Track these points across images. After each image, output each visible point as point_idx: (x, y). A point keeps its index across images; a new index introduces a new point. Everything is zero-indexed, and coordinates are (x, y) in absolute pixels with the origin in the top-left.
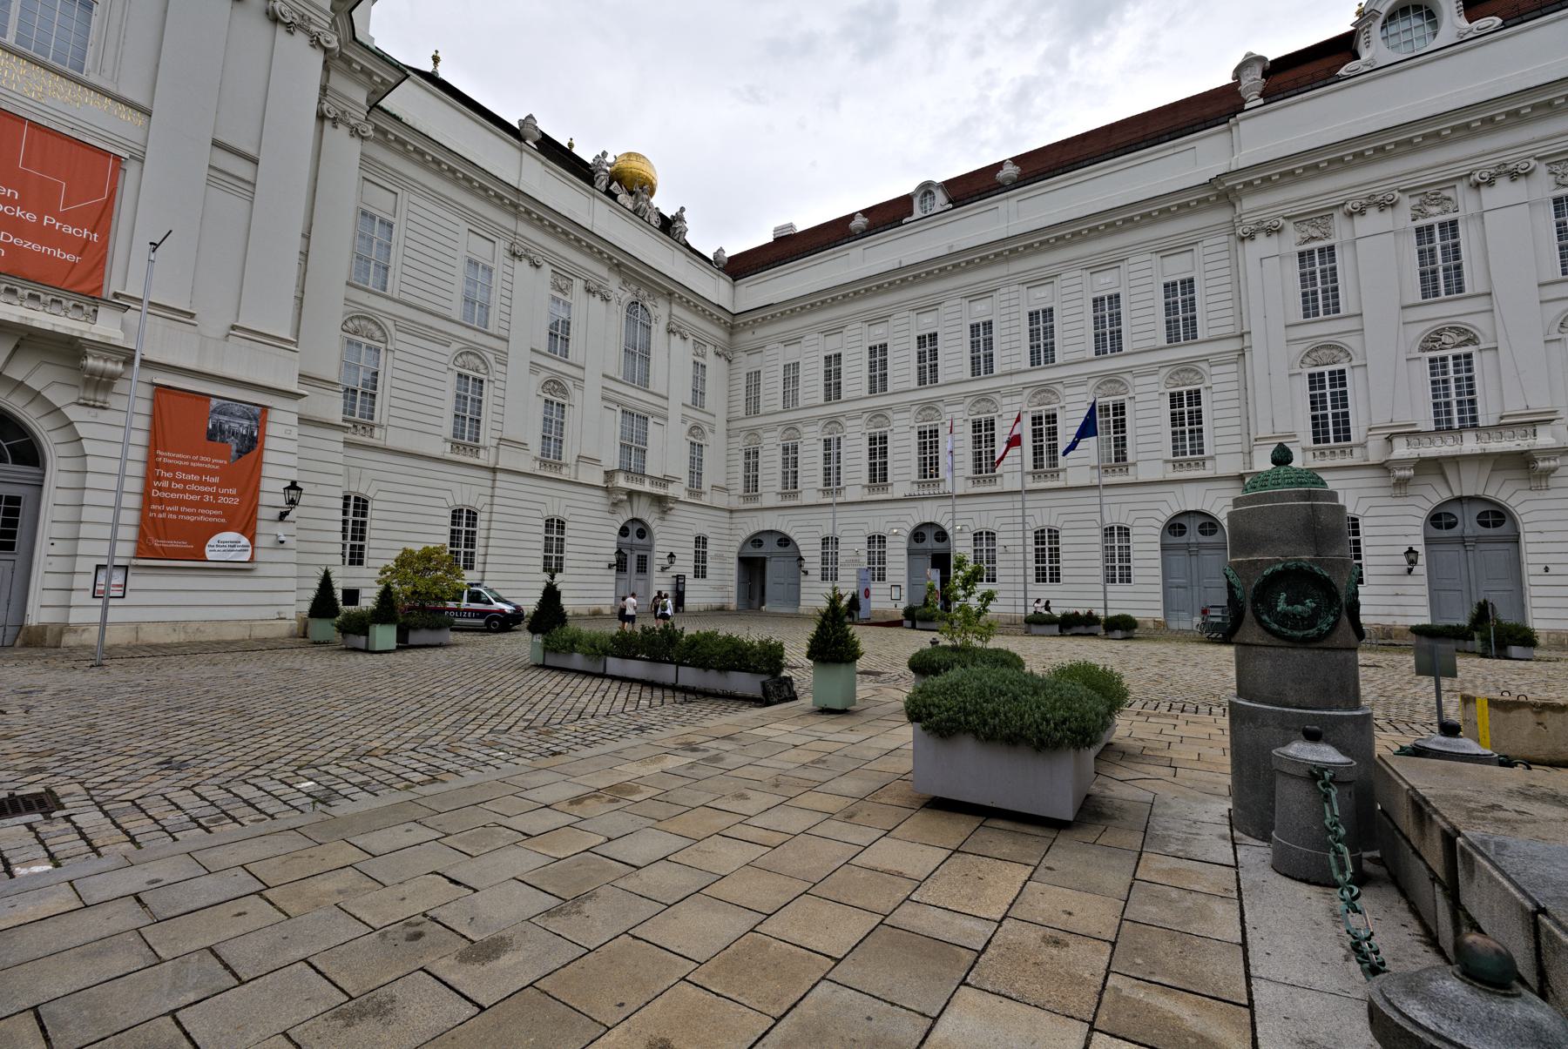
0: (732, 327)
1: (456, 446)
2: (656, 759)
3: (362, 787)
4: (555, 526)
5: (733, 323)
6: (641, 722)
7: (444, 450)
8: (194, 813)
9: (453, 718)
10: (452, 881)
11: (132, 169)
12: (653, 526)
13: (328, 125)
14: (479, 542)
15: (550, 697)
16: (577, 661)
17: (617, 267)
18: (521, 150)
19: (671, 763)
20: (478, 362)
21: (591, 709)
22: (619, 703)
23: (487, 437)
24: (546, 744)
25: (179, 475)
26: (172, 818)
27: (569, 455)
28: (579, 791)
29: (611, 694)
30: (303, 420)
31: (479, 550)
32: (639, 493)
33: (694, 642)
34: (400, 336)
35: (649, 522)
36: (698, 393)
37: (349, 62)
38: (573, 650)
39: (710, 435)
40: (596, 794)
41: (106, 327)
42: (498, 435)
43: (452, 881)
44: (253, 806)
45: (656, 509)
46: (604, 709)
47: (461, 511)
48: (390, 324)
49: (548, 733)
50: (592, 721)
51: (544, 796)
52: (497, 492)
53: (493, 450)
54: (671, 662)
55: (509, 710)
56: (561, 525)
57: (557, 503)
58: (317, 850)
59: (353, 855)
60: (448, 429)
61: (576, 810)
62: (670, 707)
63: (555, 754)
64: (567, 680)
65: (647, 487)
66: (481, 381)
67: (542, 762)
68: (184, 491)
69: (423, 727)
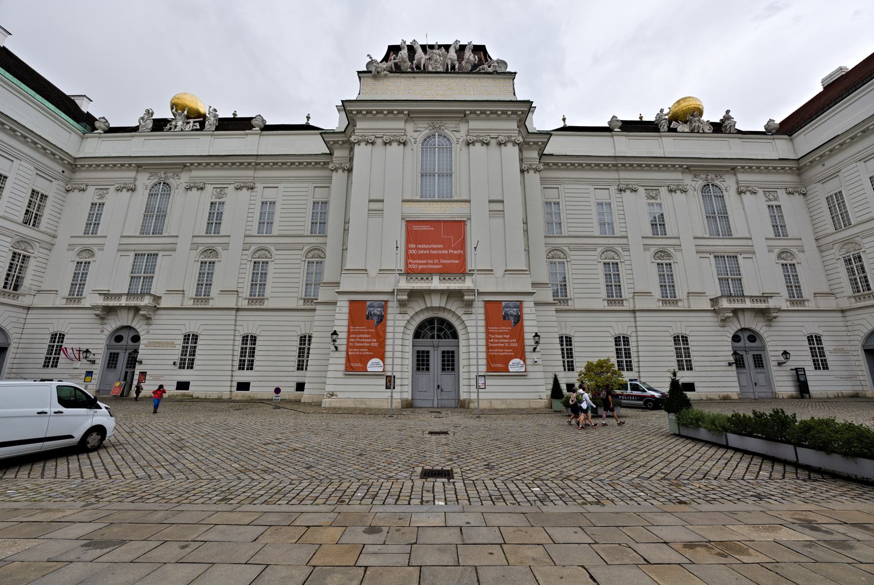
0: (799, 169)
1: (610, 302)
2: (770, 527)
3: (561, 497)
4: (681, 340)
5: (799, 167)
6: (760, 490)
7: (604, 305)
8: (491, 492)
9: (616, 464)
10: (591, 577)
11: (468, 223)
12: (761, 332)
13: (525, 173)
14: (633, 354)
15: (682, 459)
16: (703, 433)
17: (688, 169)
18: (612, 136)
19: (785, 535)
20: (613, 254)
21: (715, 472)
22: (740, 471)
23: (626, 293)
24: (676, 493)
25: (497, 336)
26: (484, 493)
27: (681, 293)
28: (693, 538)
29: (733, 463)
30: (536, 304)
31: (634, 359)
32: (743, 310)
33: (807, 427)
34: (572, 253)
35: (757, 329)
36: (779, 229)
37: (527, 143)
38: (699, 426)
39: (801, 255)
40: (707, 545)
41: (468, 284)
42: (633, 291)
43: (591, 577)
44: (512, 495)
45: (761, 319)
46: (726, 474)
47: (619, 337)
48: (566, 249)
49: (677, 485)
50: (715, 482)
51: (666, 534)
52: (638, 324)
53: (631, 300)
54: (788, 442)
55: (652, 463)
56: (685, 339)
58: (530, 530)
59: (543, 538)
60: (604, 293)
61: (688, 553)
62: (791, 482)
63: (681, 502)
64: (697, 447)
65: (748, 304)
66: (617, 264)
67: (670, 507)
68: (498, 343)
69: (598, 467)
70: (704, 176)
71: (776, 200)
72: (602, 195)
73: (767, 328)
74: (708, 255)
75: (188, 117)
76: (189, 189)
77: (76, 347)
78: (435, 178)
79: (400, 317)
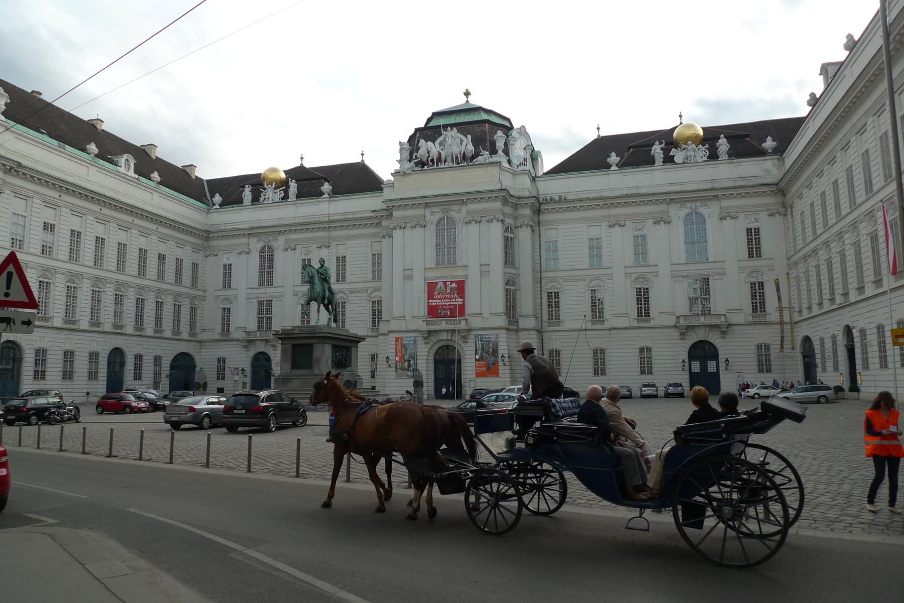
1: (593, 323)
56: (649, 350)
57: (644, 339)
70: (688, 205)
71: (756, 221)
72: (594, 232)
73: (721, 340)
74: (682, 279)
75: (275, 189)
76: (286, 250)
77: (236, 366)
78: (446, 250)
79: (425, 346)
